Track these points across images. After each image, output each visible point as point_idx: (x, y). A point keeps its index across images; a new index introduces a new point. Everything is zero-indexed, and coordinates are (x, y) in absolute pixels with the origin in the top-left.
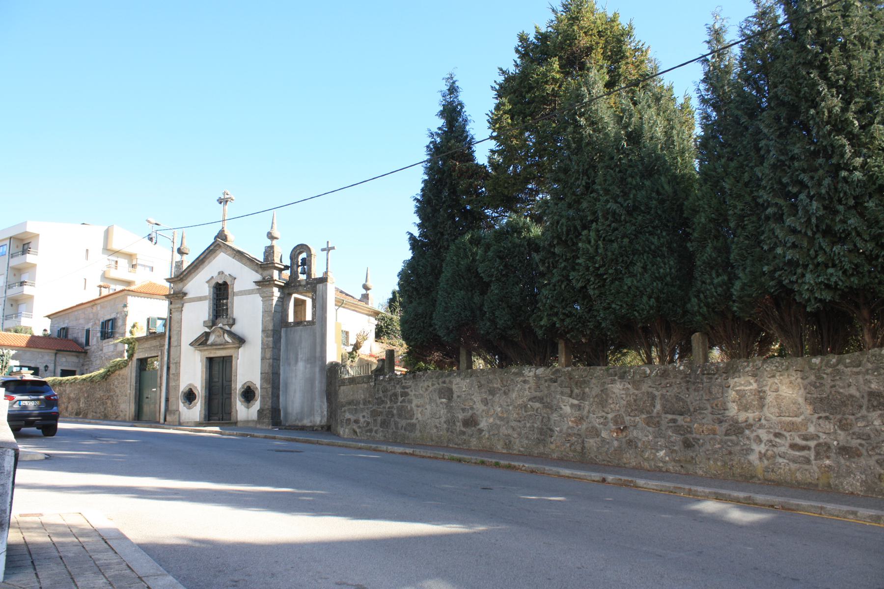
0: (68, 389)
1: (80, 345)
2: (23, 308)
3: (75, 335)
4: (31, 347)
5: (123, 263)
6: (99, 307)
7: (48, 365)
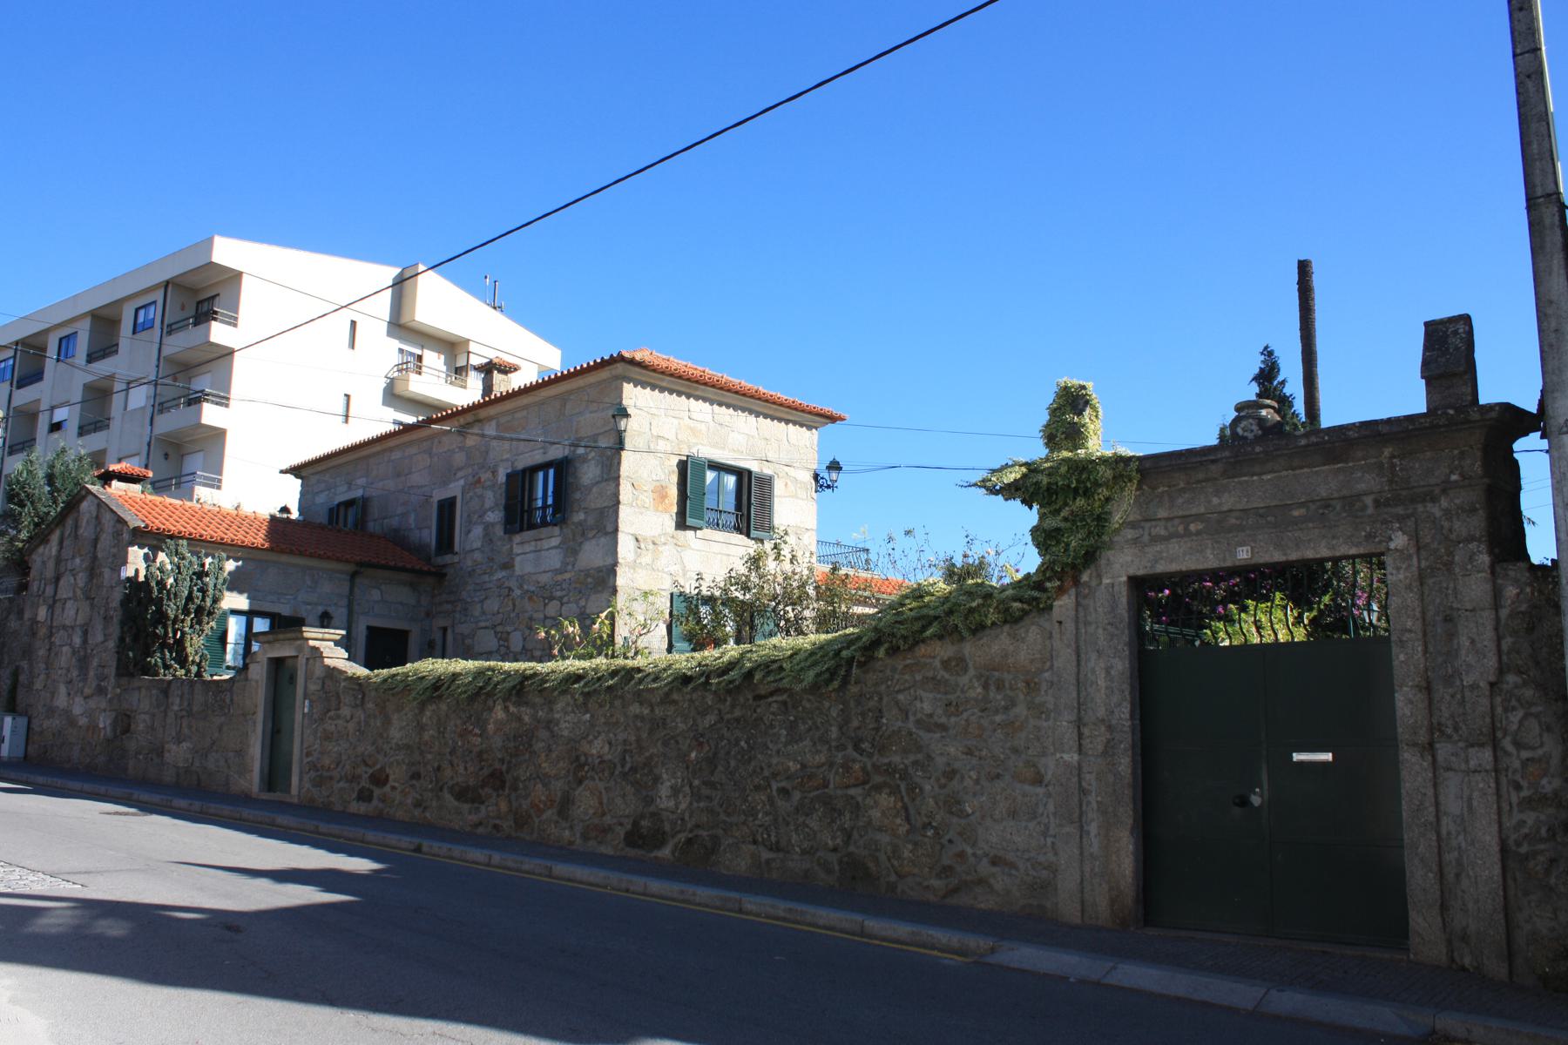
0: (567, 721)
1: (419, 550)
2: (194, 463)
3: (395, 522)
4: (282, 552)
5: (434, 360)
6: (490, 430)
7: (330, 610)
